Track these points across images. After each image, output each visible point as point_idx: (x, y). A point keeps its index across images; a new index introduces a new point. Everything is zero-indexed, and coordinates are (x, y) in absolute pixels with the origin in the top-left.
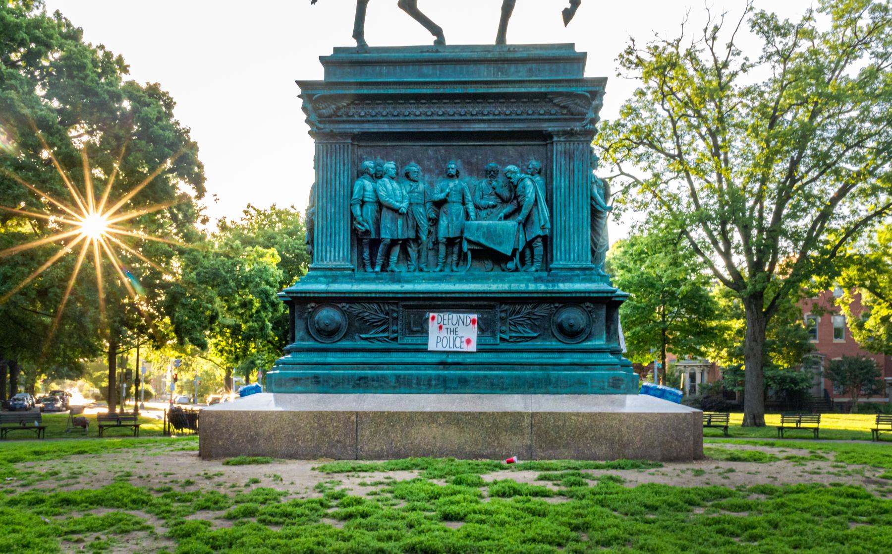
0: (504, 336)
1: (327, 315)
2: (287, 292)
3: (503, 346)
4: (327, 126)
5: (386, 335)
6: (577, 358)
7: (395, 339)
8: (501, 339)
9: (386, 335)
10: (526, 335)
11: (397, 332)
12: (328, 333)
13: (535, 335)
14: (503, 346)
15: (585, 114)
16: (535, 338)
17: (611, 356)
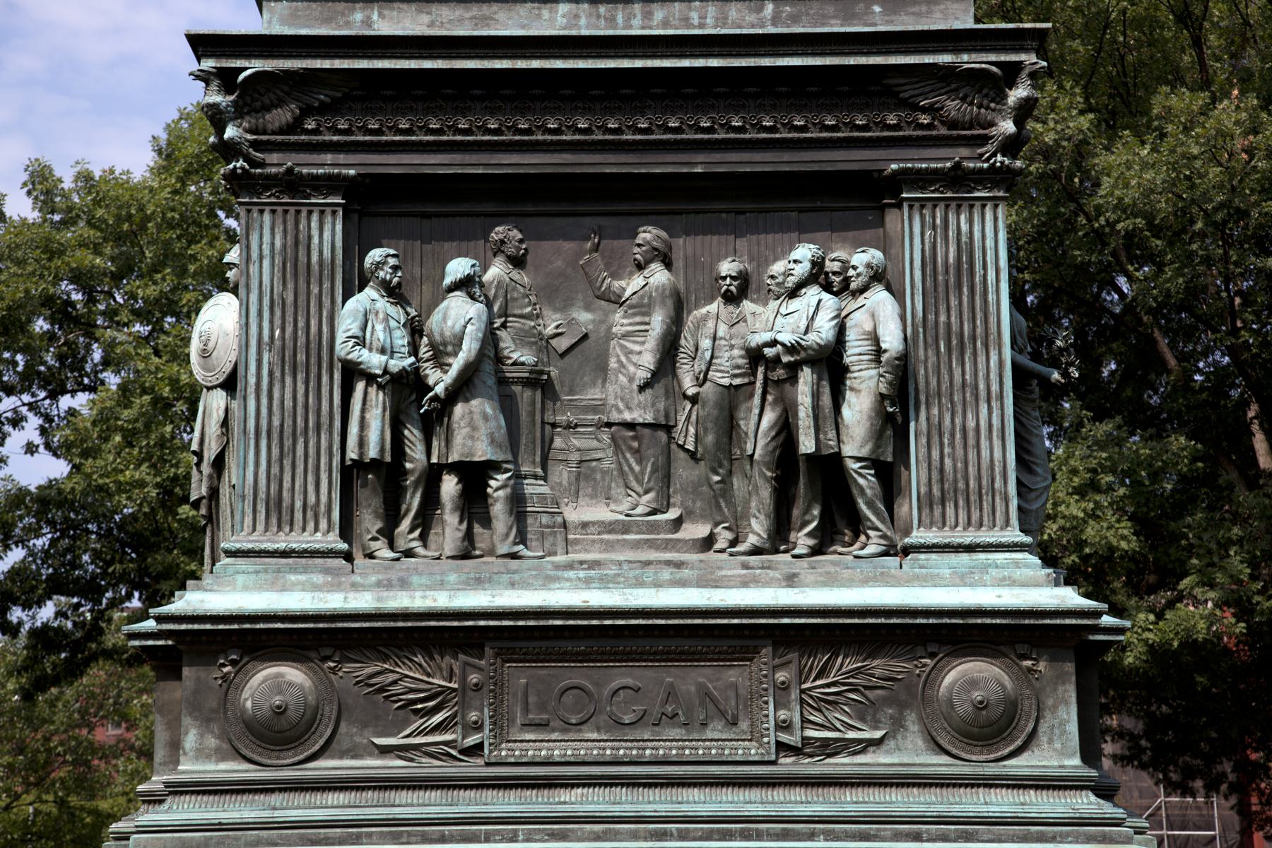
0: (784, 737)
1: (277, 682)
2: (160, 619)
3: (787, 764)
4: (274, 158)
5: (448, 737)
6: (1000, 803)
7: (476, 750)
8: (781, 746)
9: (448, 737)
10: (851, 735)
11: (478, 727)
12: (277, 734)
13: (878, 734)
14: (787, 764)
15: (992, 124)
16: (878, 743)
17: (1093, 798)
